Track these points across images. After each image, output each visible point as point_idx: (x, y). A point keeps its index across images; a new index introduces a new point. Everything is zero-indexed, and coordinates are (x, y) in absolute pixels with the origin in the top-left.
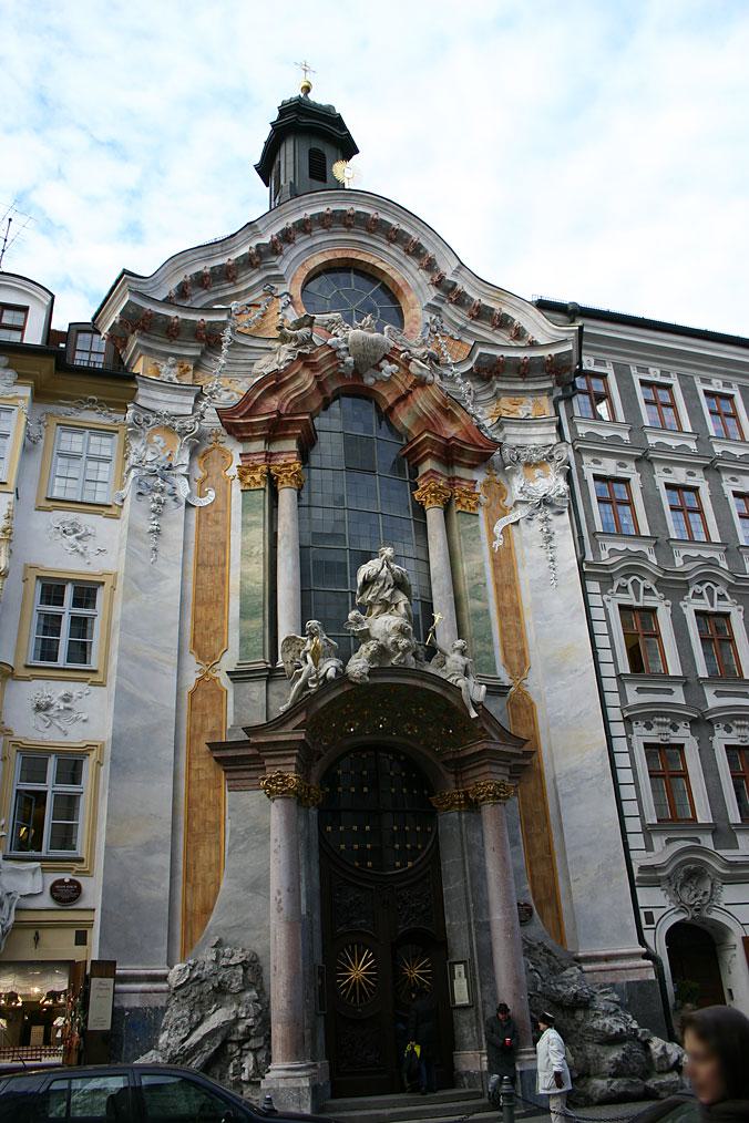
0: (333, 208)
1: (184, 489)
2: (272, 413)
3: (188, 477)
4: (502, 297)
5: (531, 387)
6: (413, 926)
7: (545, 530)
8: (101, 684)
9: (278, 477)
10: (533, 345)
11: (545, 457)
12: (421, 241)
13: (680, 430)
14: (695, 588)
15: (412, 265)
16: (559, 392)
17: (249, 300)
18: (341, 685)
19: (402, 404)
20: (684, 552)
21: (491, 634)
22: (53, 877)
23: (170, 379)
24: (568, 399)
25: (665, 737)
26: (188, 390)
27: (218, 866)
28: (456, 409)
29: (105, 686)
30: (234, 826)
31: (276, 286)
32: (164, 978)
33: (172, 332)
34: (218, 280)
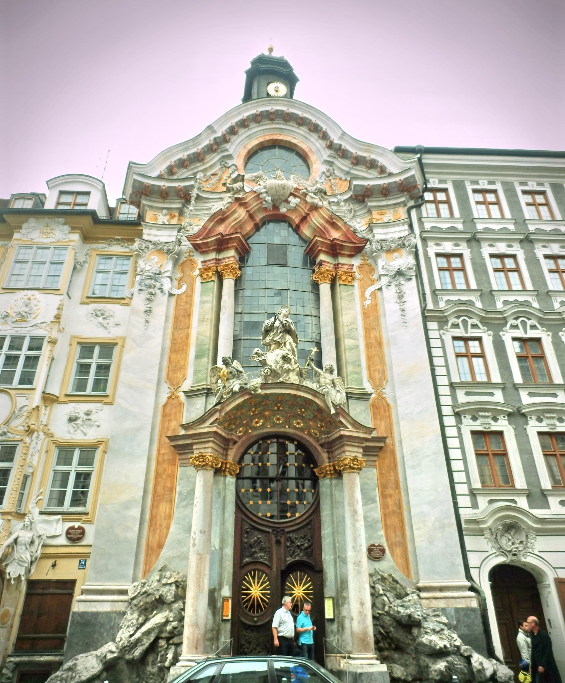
0: (261, 109)
1: (167, 285)
2: (217, 235)
3: (170, 277)
4: (370, 148)
5: (391, 202)
6: (297, 558)
7: (398, 291)
8: (110, 404)
9: (222, 273)
10: (391, 175)
11: (399, 245)
12: (318, 122)
13: (503, 218)
14: (511, 322)
15: (314, 137)
16: (412, 203)
17: (212, 172)
18: (243, 395)
19: (304, 223)
20: (503, 299)
21: (359, 360)
22: (69, 525)
23: (163, 222)
24: (418, 207)
25: (487, 426)
27: (169, 517)
28: (338, 221)
29: (112, 404)
30: (181, 489)
31: (228, 161)
32: (124, 592)
33: (164, 195)
34: (194, 162)
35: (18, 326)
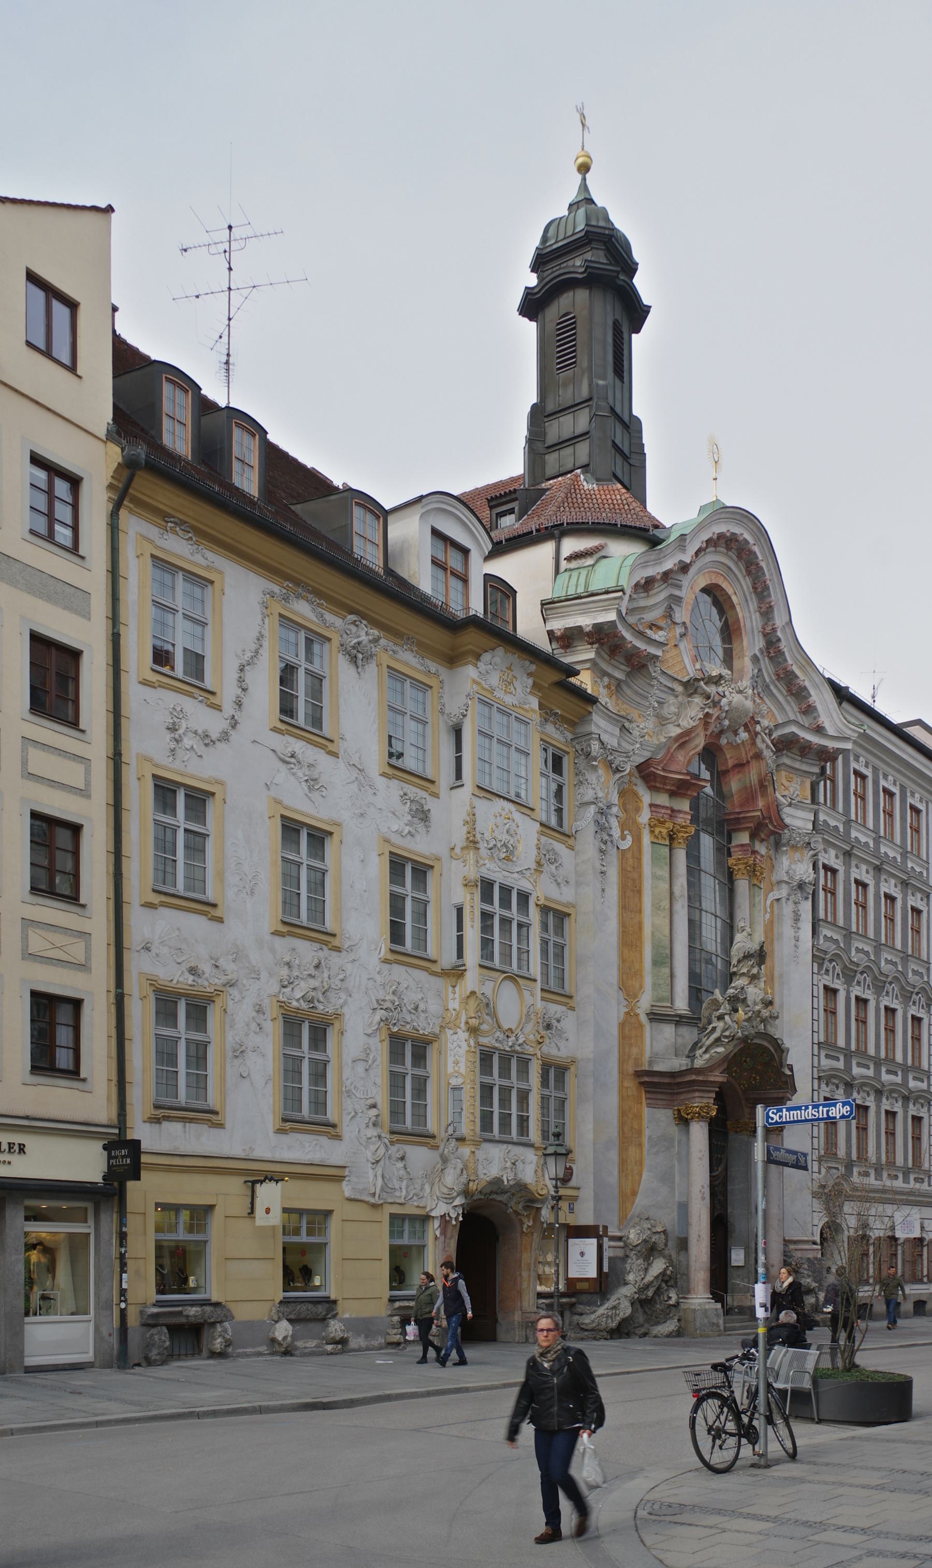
26: (618, 721)
35: (504, 867)
